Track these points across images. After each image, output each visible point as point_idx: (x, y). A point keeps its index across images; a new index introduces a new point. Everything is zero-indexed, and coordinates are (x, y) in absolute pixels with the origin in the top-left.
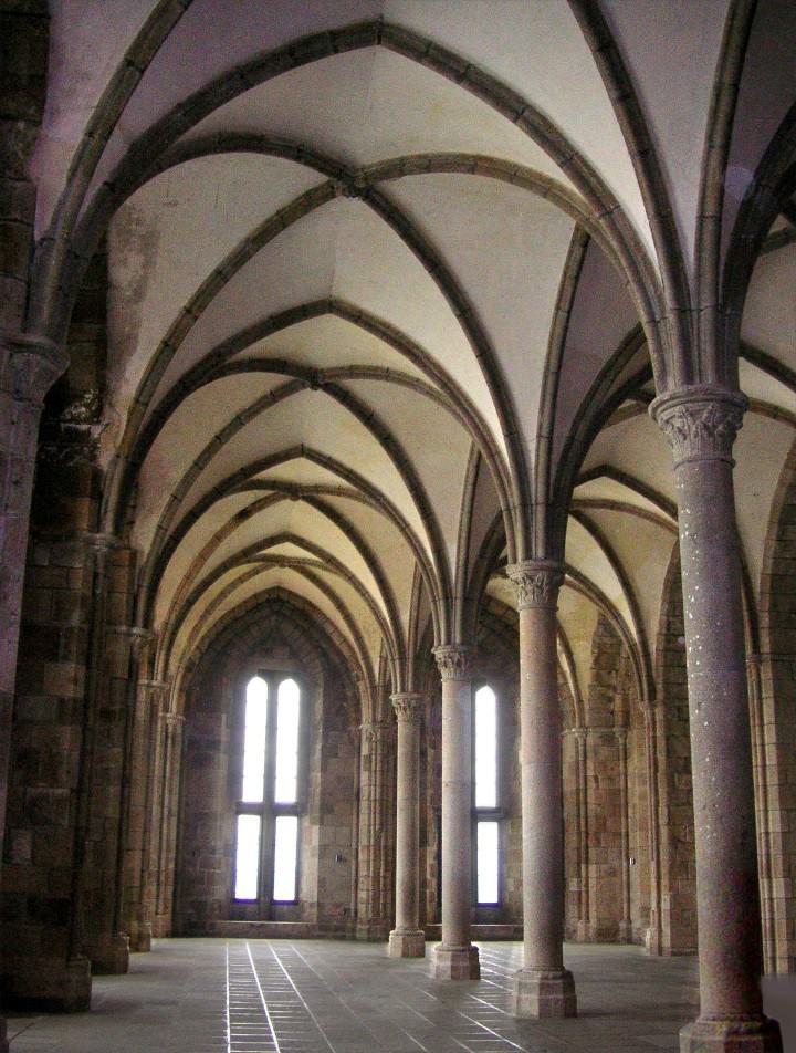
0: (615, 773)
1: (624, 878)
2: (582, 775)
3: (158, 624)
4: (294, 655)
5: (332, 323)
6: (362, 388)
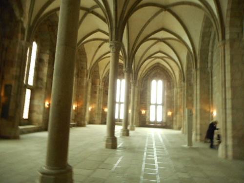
3: (88, 68)
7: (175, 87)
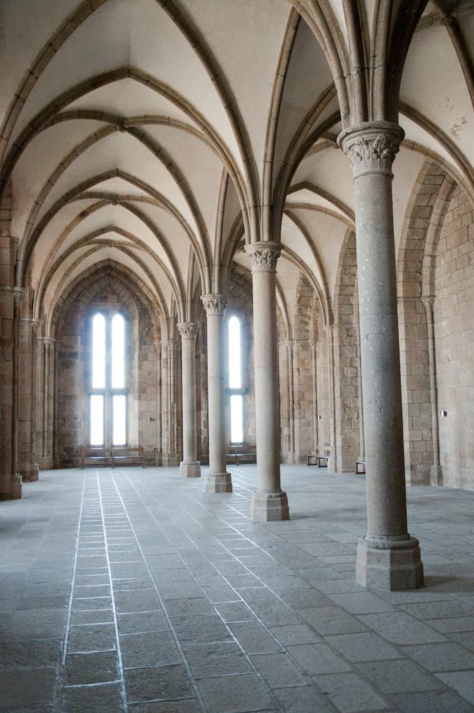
0: (309, 367)
1: (315, 427)
2: (290, 367)
3: (34, 284)
4: (119, 300)
5: (131, 84)
6: (152, 130)
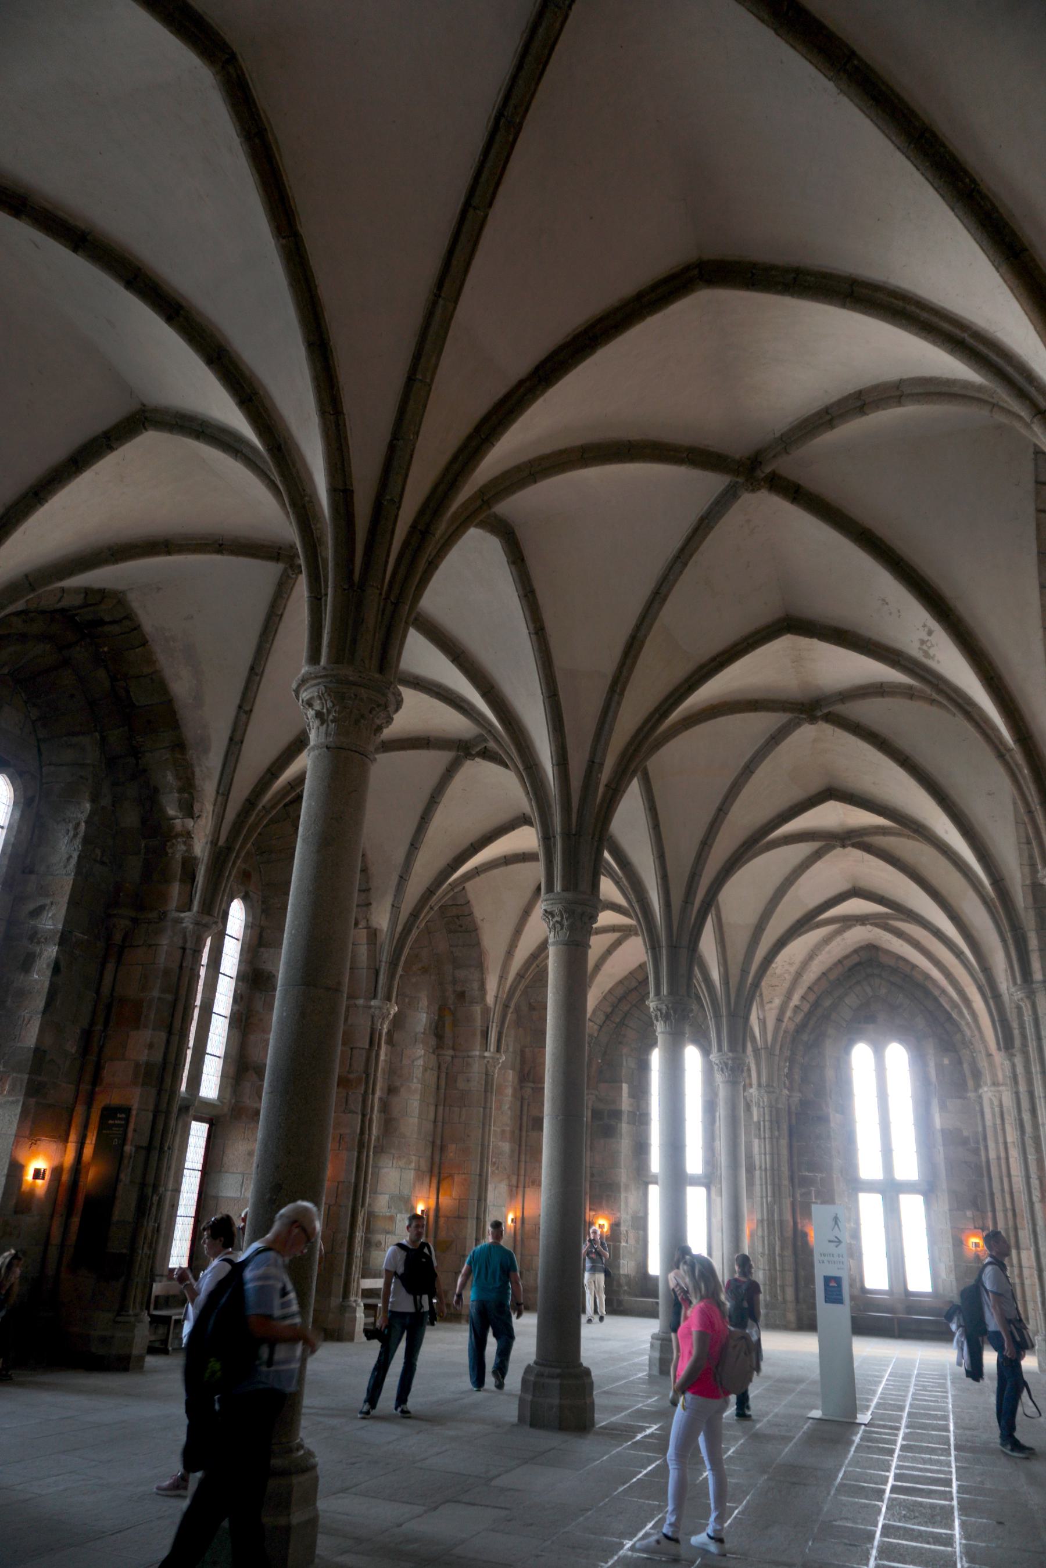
2: (1001, 1140)
3: (490, 999)
7: (987, 1077)
